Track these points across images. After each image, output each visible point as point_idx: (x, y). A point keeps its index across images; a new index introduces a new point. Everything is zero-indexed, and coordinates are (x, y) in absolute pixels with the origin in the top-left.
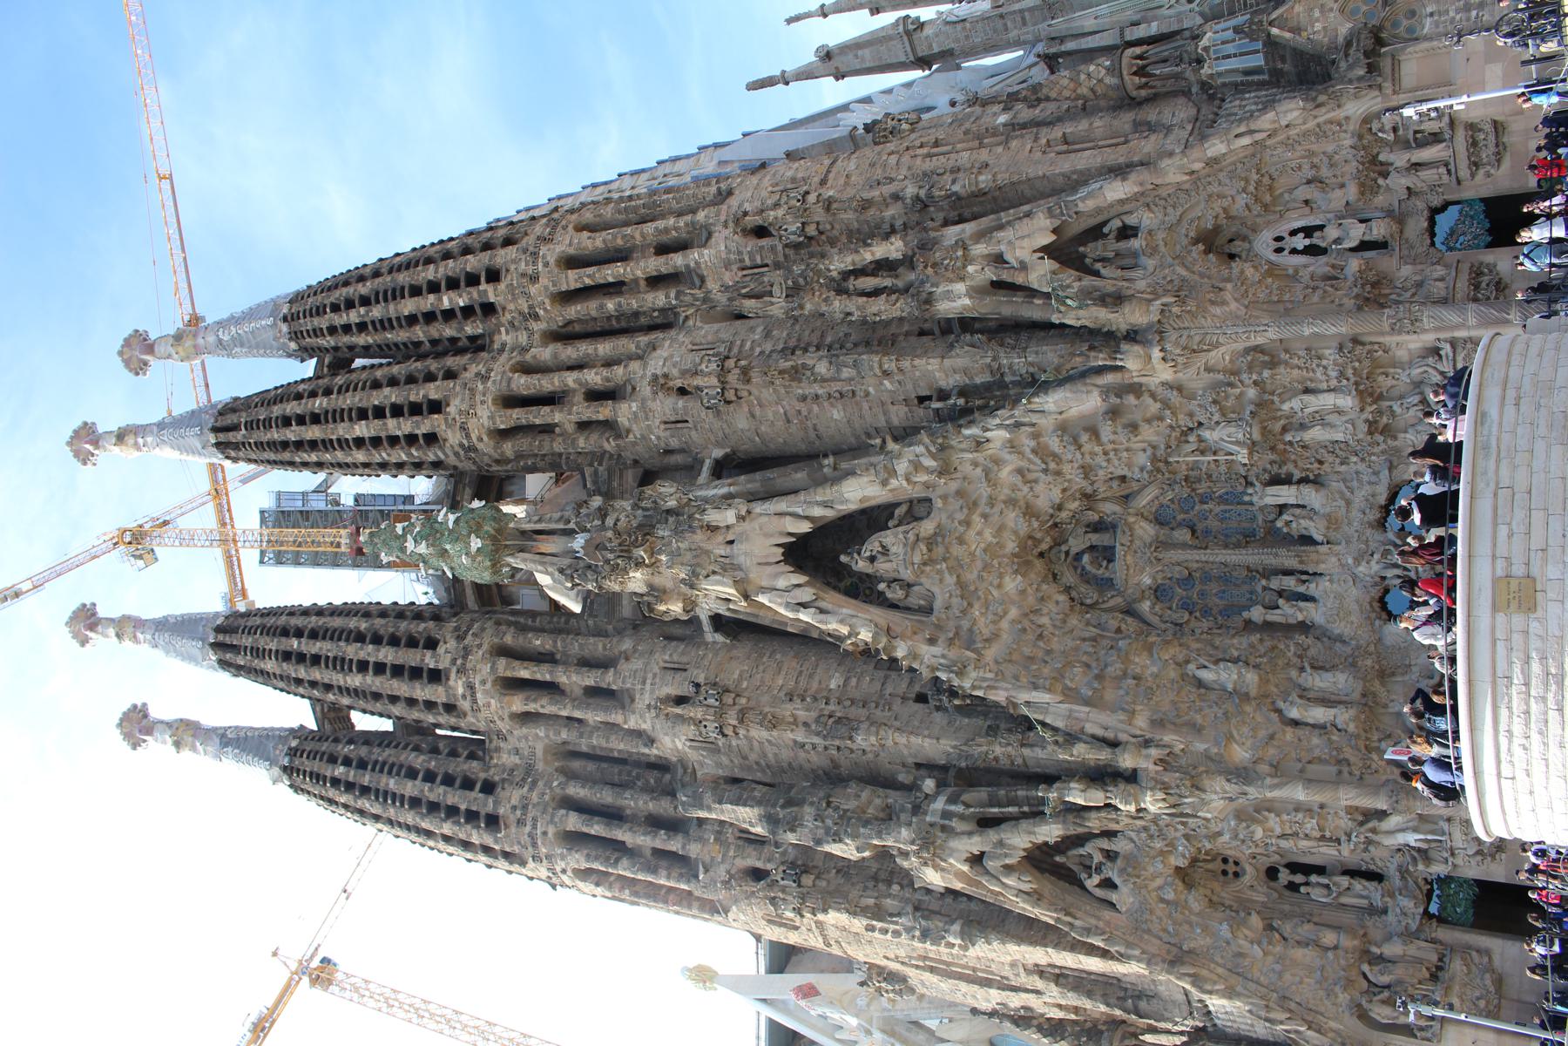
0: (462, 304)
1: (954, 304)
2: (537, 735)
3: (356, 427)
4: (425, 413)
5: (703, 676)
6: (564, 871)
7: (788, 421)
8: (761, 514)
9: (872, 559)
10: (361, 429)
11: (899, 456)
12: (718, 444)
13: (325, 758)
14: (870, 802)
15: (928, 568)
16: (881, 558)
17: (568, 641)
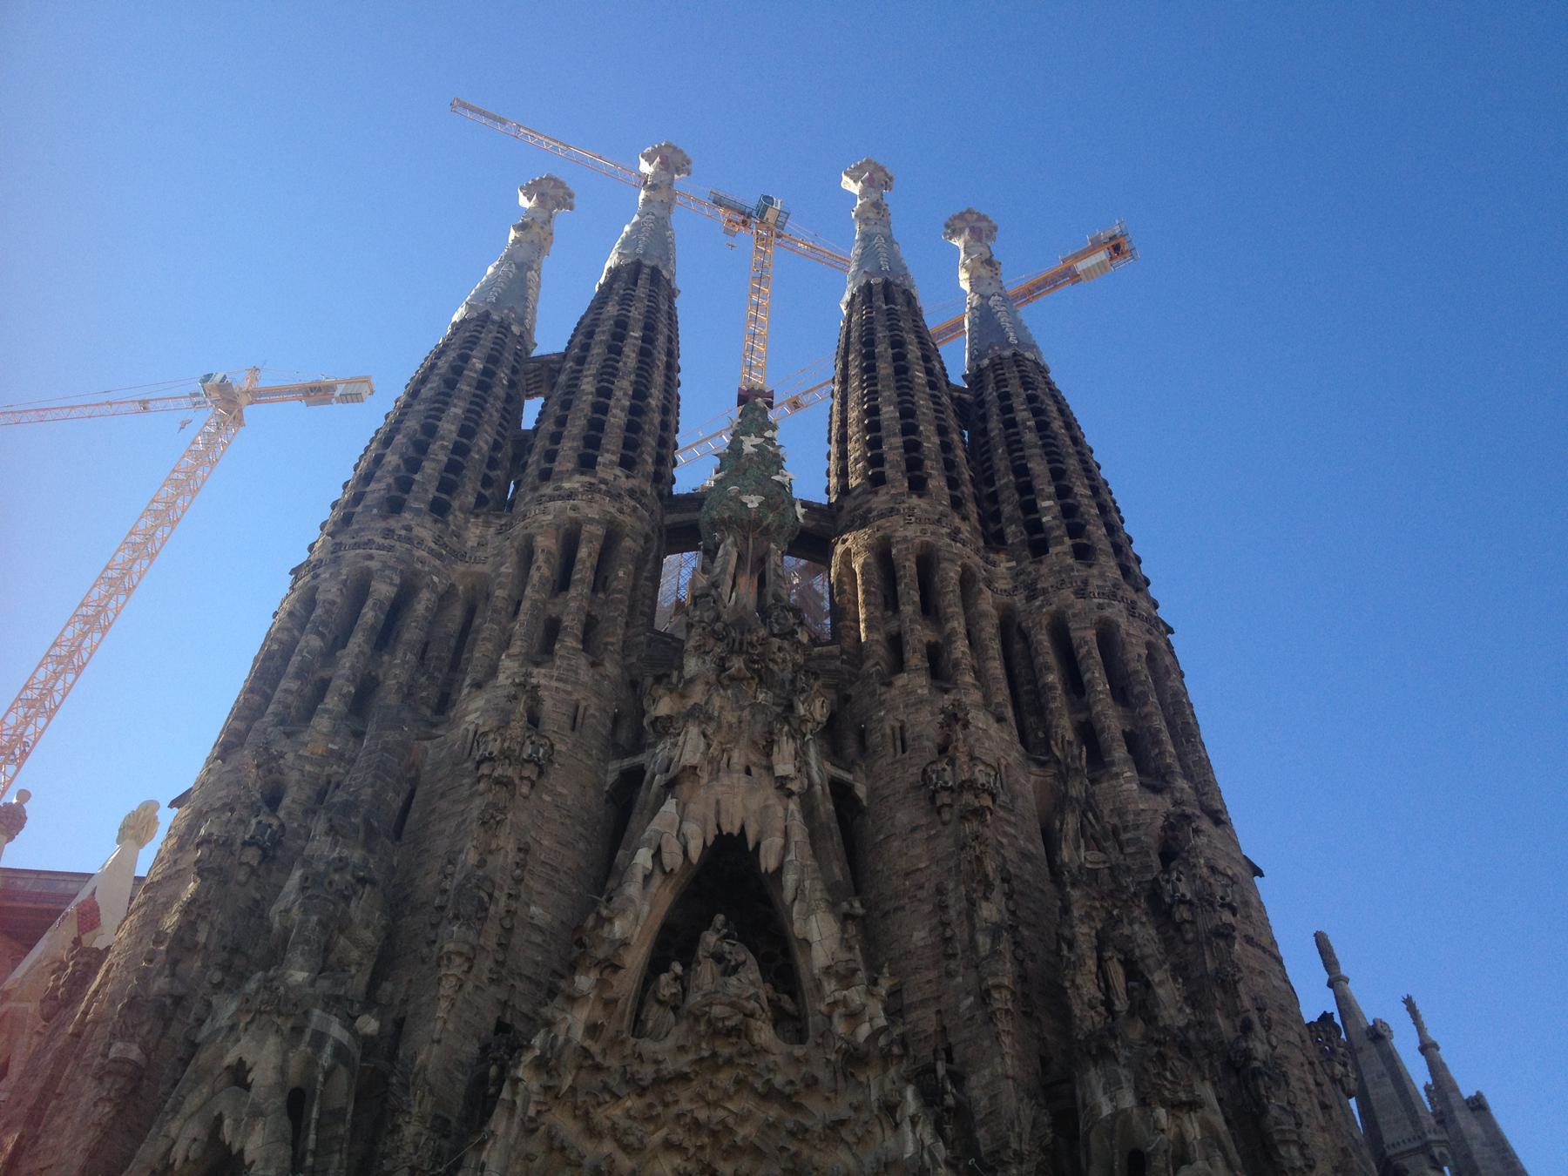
0: (1044, 519)
1: (1100, 1093)
2: (502, 564)
3: (892, 408)
4: (909, 474)
5: (564, 749)
6: (316, 577)
7: (907, 874)
8: (786, 809)
9: (718, 957)
10: (889, 412)
11: (870, 993)
12: (872, 792)
13: (495, 353)
14: (356, 943)
15: (702, 1028)
16: (717, 969)
17: (621, 607)
